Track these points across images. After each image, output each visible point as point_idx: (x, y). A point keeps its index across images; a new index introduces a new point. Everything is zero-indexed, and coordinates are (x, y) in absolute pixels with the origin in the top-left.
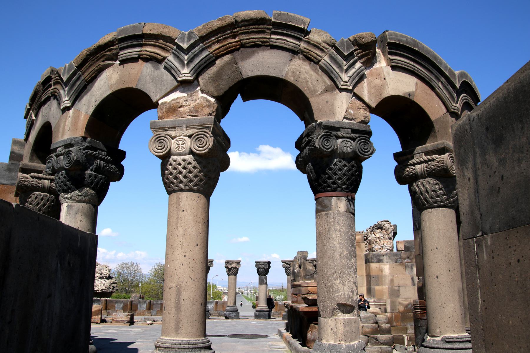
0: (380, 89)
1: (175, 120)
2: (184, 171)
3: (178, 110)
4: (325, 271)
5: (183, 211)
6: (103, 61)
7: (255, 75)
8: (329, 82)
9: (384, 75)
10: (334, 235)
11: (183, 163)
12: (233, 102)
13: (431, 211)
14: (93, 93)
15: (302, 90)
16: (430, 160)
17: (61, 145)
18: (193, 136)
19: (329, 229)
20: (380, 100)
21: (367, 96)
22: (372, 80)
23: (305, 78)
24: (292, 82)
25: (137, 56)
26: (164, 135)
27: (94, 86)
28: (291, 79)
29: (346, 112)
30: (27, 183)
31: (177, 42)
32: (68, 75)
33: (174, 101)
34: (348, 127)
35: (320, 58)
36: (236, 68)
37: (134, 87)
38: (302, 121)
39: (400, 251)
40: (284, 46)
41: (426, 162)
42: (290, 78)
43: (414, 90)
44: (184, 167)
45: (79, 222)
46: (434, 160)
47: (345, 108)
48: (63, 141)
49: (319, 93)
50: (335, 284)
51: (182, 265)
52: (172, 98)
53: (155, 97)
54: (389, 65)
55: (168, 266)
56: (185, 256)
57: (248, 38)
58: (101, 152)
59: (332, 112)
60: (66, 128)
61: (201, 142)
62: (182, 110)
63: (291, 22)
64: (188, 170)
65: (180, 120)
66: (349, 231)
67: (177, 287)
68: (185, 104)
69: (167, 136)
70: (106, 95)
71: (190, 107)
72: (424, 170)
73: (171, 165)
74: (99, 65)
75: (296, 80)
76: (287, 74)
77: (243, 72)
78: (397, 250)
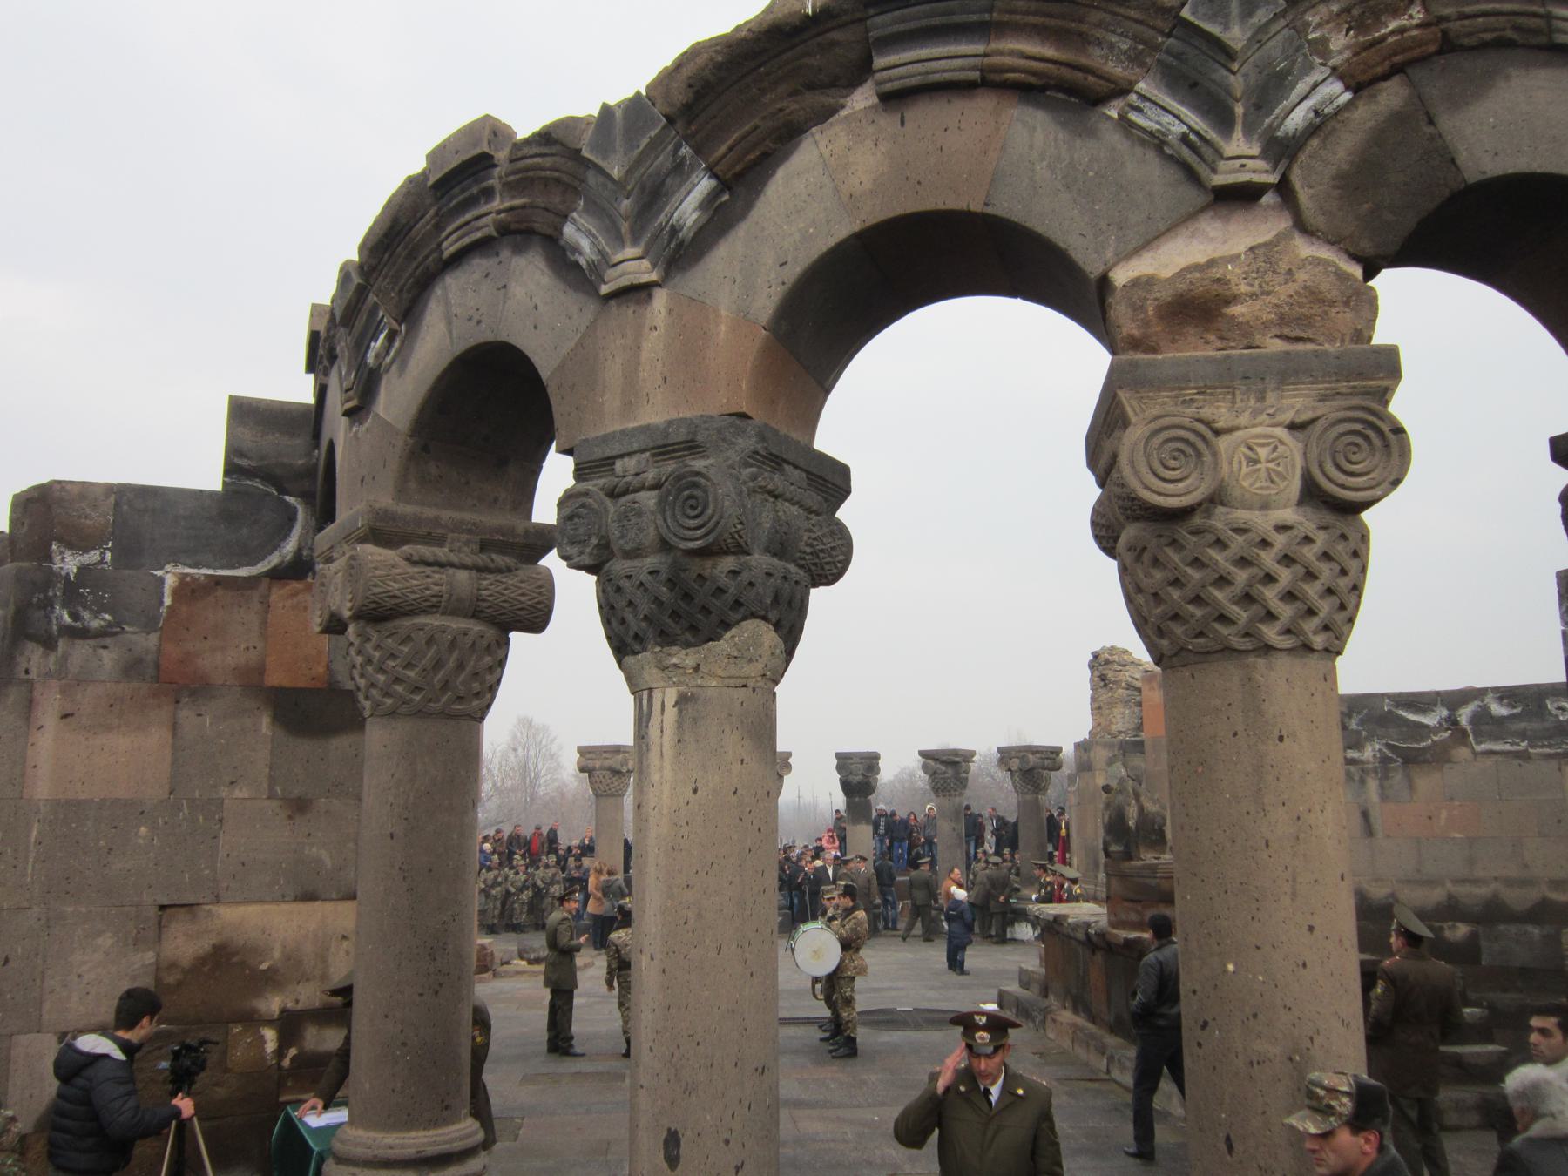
2: (1285, 576)
3: (1223, 315)
5: (1281, 739)
7: (1510, 171)
11: (1280, 540)
14: (763, 229)
17: (635, 447)
25: (976, 75)
26: (1186, 422)
27: (762, 198)
30: (396, 586)
31: (1192, 19)
33: (1197, 275)
36: (1432, 138)
37: (972, 208)
44: (1286, 556)
45: (737, 767)
48: (646, 429)
51: (1304, 965)
52: (1182, 262)
55: (1231, 967)
56: (1311, 929)
57: (1468, 10)
60: (644, 374)
62: (1242, 314)
67: (1291, 1059)
73: (1220, 544)
74: (781, 110)
77: (1463, 158)
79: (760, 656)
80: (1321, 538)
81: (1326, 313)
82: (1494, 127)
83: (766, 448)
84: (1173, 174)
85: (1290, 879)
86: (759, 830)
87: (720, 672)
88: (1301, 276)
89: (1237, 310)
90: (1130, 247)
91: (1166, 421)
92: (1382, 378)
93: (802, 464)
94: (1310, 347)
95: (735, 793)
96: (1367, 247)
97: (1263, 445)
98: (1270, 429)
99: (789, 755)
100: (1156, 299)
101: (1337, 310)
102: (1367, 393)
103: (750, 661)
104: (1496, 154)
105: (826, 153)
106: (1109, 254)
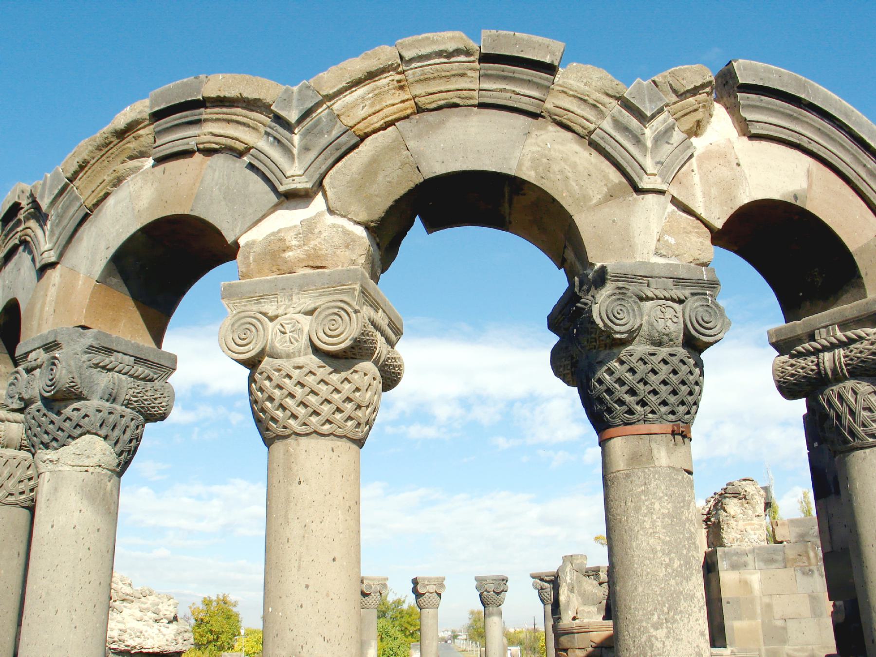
0: (728, 188)
1: (276, 279)
2: (299, 391)
3: (281, 257)
4: (633, 607)
5: (300, 483)
6: (123, 162)
8: (615, 176)
9: (736, 155)
10: (647, 525)
11: (296, 373)
12: (405, 234)
13: (863, 455)
14: (102, 231)
15: (556, 197)
16: (851, 341)
17: (36, 346)
18: (316, 313)
19: (637, 509)
20: (731, 212)
21: (701, 204)
22: (711, 169)
23: (561, 172)
26: (252, 314)
28: (529, 175)
29: (659, 240)
31: (276, 110)
32: (50, 193)
34: (666, 275)
35: (592, 127)
38: (559, 269)
39: (781, 542)
41: (842, 344)
42: (527, 172)
43: (805, 185)
46: (861, 339)
47: (655, 233)
49: (594, 201)
50: (657, 639)
51: (301, 606)
53: (233, 230)
54: (744, 135)
55: (270, 610)
56: (307, 586)
58: (122, 358)
59: (627, 242)
61: (333, 325)
62: (289, 256)
63: (522, 51)
64: (307, 390)
65: (287, 279)
66: (683, 512)
68: (297, 243)
71: (306, 248)
72: (840, 363)
75: (542, 178)
76: (520, 165)
79: (95, 455)
81: (335, 253)
82: (443, 149)
83: (99, 344)
85: (298, 559)
86: (89, 549)
87: (70, 463)
89: (289, 254)
91: (242, 315)
92: (350, 285)
93: (131, 353)
95: (74, 528)
97: (288, 324)
98: (294, 315)
99: (444, 579)
100: (254, 252)
101: (341, 250)
103: (88, 457)
104: (443, 162)
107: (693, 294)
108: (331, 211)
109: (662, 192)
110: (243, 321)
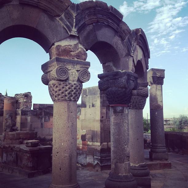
10: (125, 125)
19: (123, 122)
24: (115, 48)
28: (115, 47)
33: (67, 47)
37: (35, 27)
39: (35, 109)
40: (114, 27)
49: (124, 56)
54: (138, 45)
55: (62, 144)
59: (128, 68)
69: (66, 69)
70: (9, 26)
77: (98, 38)
78: (33, 109)
80: (79, 86)
84: (64, 31)
88: (80, 50)
89: (72, 53)
90: (58, 40)
91: (63, 67)
94: (79, 60)
96: (87, 48)
102: (86, 68)
105: (9, 9)
106: (55, 40)
107: (135, 80)
108: (81, 44)
109: (132, 56)
110: (61, 69)
